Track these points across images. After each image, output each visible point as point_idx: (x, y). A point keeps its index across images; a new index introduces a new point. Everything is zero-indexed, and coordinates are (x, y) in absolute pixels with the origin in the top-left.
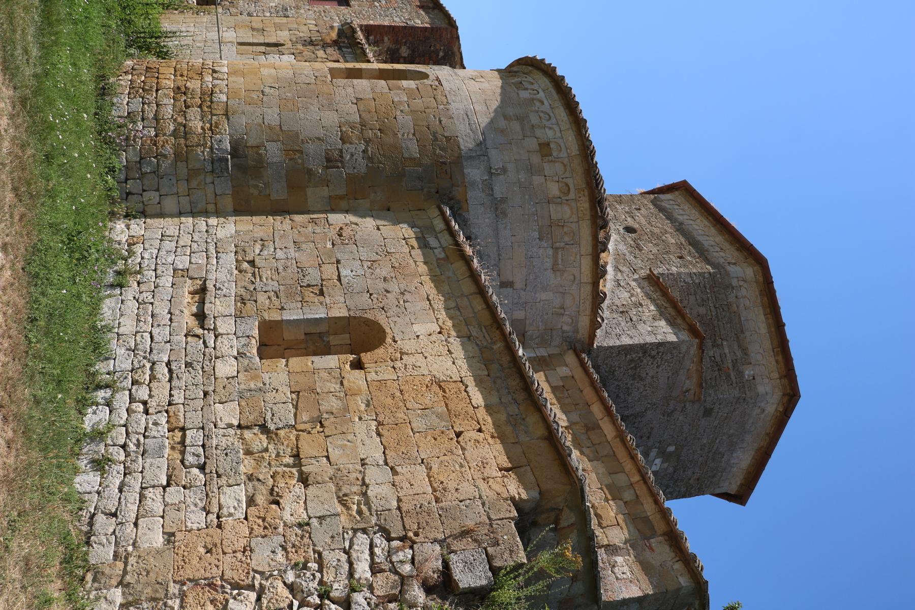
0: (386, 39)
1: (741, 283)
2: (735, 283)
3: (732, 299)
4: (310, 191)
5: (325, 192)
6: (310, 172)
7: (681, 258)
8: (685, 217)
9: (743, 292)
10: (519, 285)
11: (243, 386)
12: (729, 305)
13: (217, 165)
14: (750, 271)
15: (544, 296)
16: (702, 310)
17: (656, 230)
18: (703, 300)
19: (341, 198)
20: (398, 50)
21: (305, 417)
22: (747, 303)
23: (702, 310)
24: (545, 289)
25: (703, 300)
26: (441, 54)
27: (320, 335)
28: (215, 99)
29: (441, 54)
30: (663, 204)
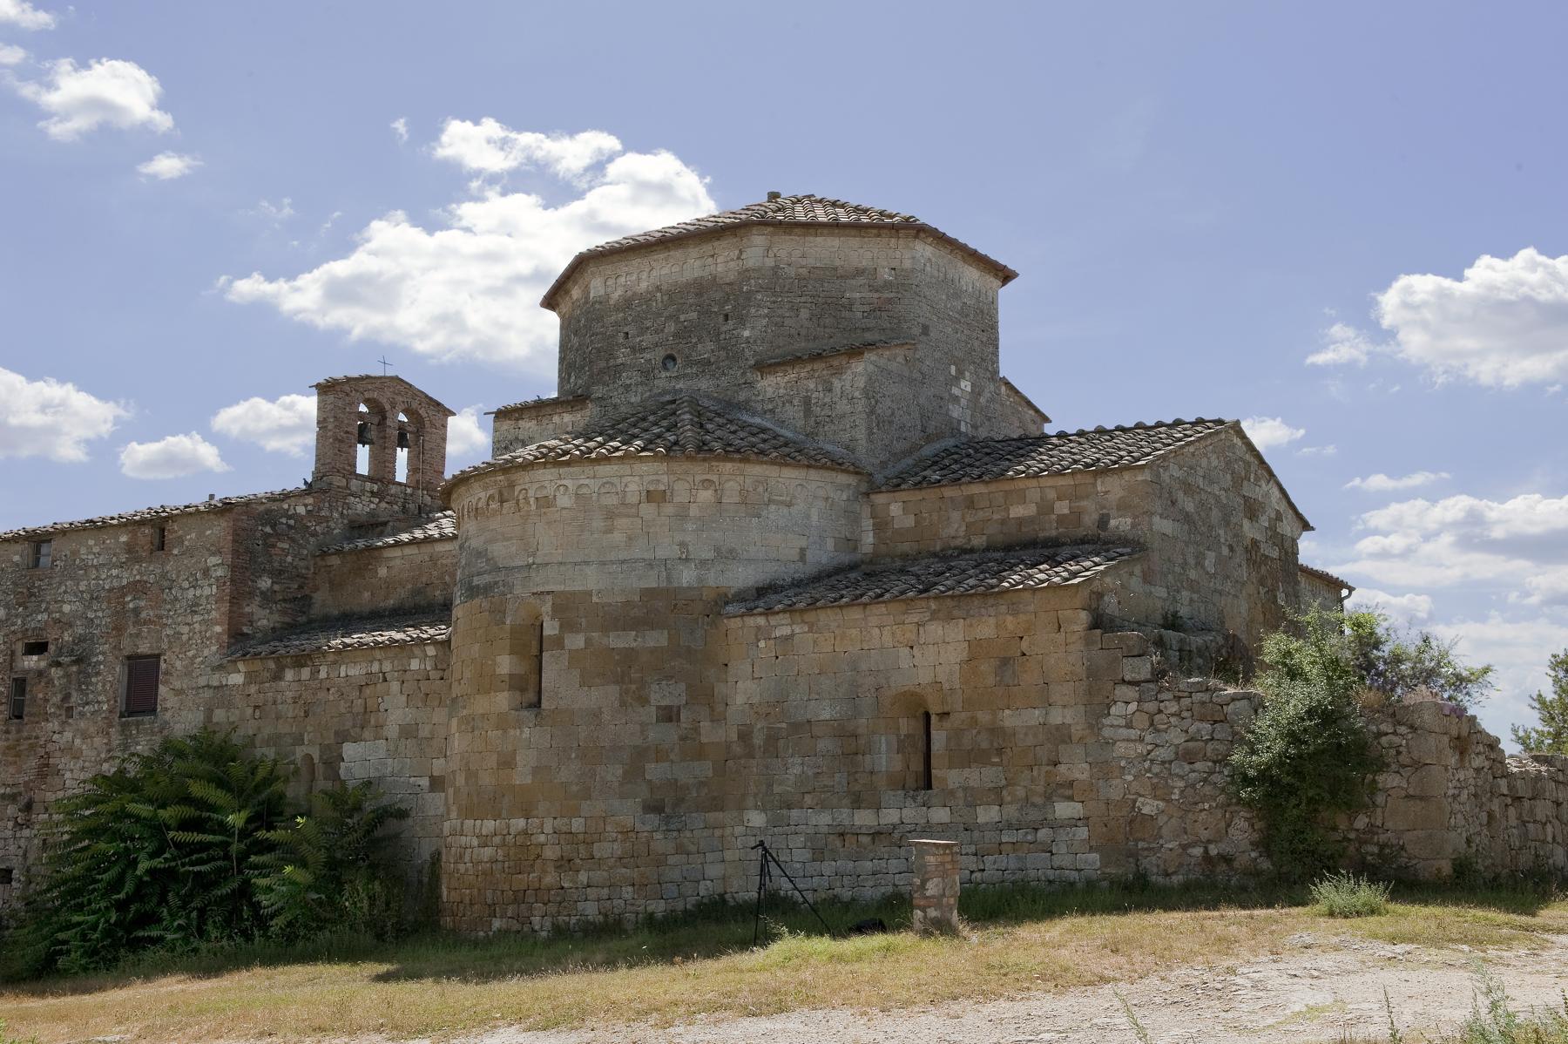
0: (247, 609)
1: (771, 254)
2: (770, 262)
3: (792, 272)
4: (704, 740)
5: (705, 725)
6: (683, 739)
7: (726, 317)
8: (644, 276)
9: (783, 254)
10: (803, 543)
11: (961, 802)
12: (799, 278)
13: (672, 827)
14: (758, 240)
15: (815, 518)
16: (804, 314)
17: (671, 327)
18: (791, 309)
19: (712, 709)
20: (262, 593)
21: (996, 760)
22: (797, 253)
23: (804, 314)
24: (808, 517)
25: (791, 309)
26: (268, 529)
27: (899, 741)
28: (582, 829)
29: (268, 529)
30: (616, 296)
